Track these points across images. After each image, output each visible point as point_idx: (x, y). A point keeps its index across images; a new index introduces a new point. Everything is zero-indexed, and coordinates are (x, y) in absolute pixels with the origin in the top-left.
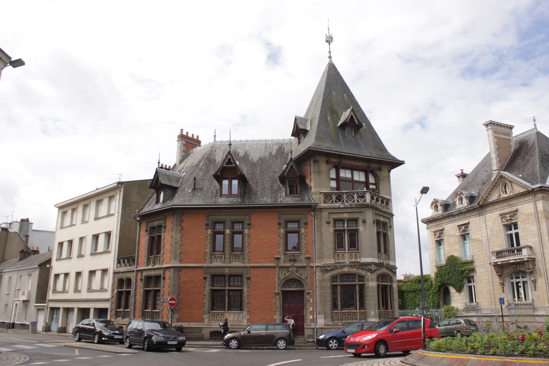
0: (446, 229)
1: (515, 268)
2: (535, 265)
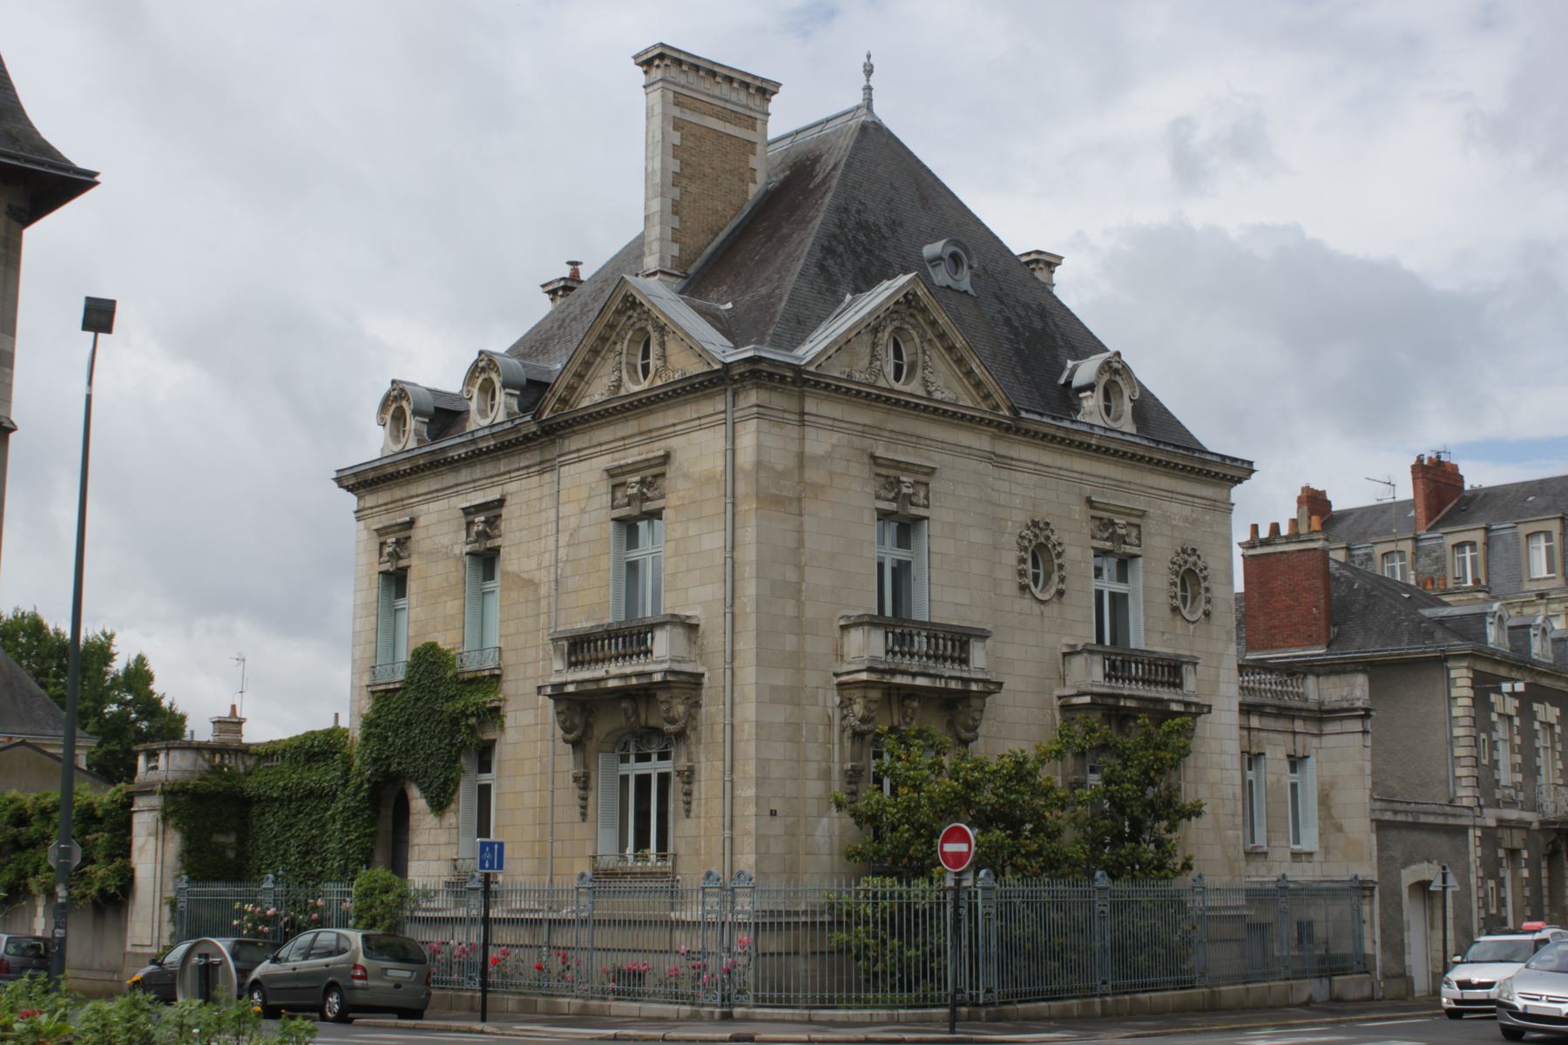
0: (422, 522)
1: (630, 712)
2: (697, 705)
